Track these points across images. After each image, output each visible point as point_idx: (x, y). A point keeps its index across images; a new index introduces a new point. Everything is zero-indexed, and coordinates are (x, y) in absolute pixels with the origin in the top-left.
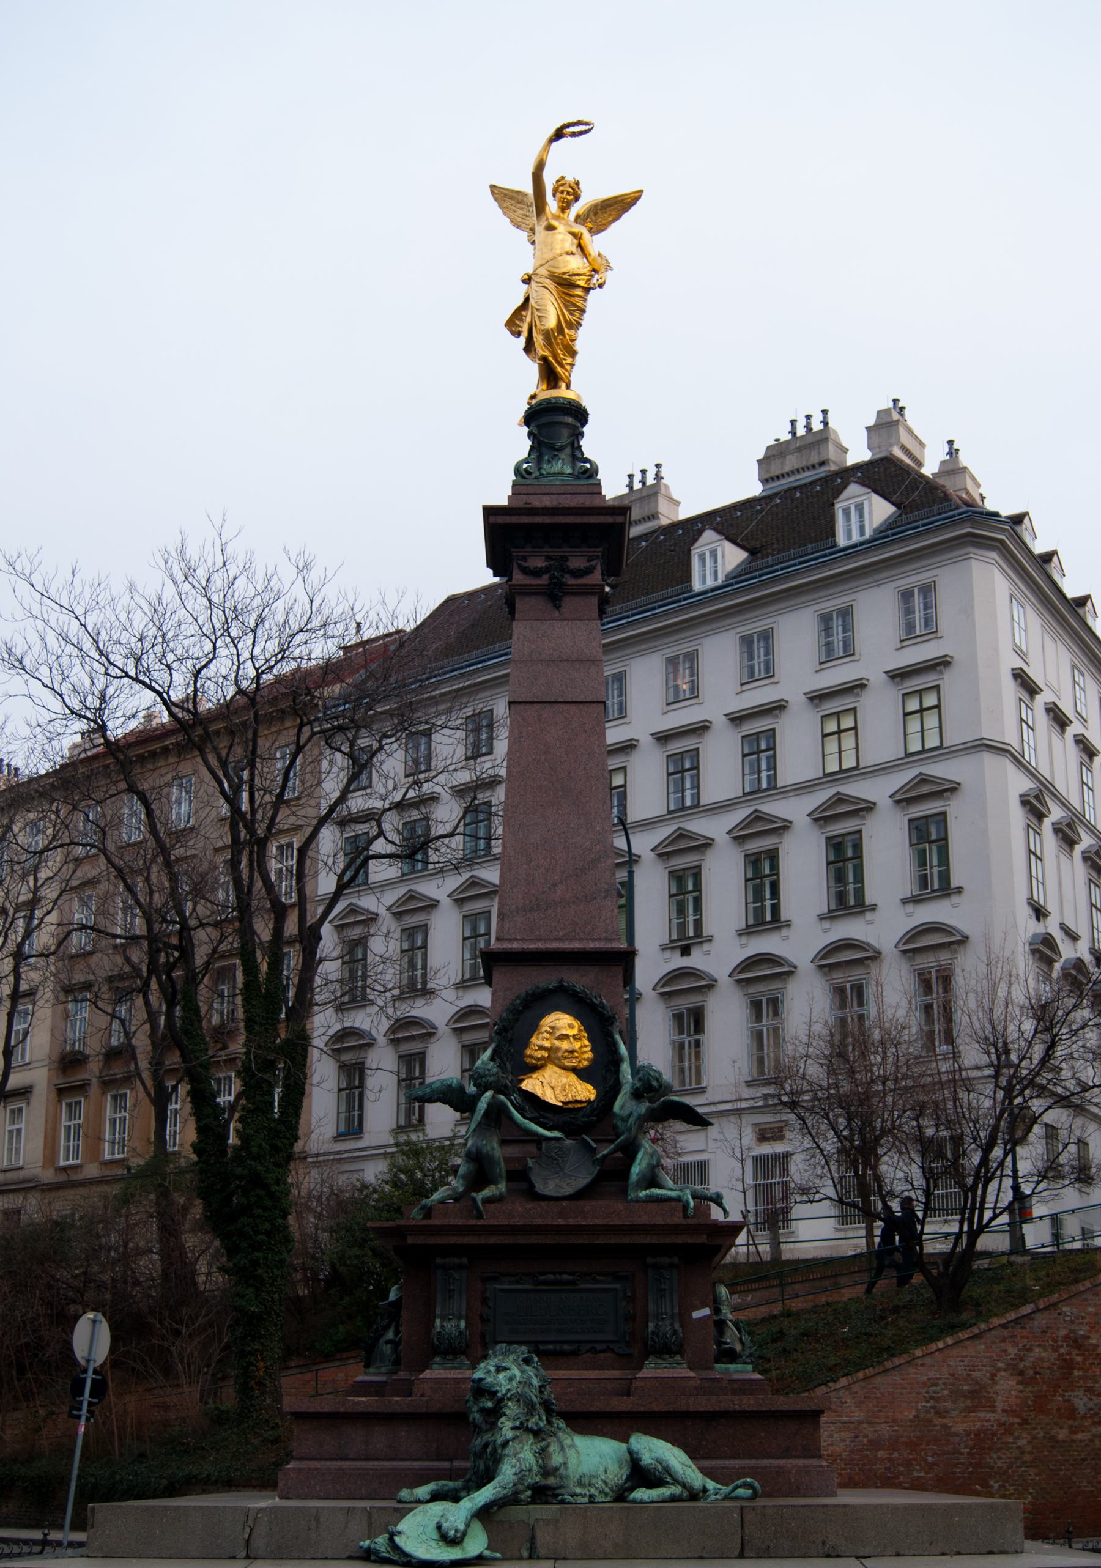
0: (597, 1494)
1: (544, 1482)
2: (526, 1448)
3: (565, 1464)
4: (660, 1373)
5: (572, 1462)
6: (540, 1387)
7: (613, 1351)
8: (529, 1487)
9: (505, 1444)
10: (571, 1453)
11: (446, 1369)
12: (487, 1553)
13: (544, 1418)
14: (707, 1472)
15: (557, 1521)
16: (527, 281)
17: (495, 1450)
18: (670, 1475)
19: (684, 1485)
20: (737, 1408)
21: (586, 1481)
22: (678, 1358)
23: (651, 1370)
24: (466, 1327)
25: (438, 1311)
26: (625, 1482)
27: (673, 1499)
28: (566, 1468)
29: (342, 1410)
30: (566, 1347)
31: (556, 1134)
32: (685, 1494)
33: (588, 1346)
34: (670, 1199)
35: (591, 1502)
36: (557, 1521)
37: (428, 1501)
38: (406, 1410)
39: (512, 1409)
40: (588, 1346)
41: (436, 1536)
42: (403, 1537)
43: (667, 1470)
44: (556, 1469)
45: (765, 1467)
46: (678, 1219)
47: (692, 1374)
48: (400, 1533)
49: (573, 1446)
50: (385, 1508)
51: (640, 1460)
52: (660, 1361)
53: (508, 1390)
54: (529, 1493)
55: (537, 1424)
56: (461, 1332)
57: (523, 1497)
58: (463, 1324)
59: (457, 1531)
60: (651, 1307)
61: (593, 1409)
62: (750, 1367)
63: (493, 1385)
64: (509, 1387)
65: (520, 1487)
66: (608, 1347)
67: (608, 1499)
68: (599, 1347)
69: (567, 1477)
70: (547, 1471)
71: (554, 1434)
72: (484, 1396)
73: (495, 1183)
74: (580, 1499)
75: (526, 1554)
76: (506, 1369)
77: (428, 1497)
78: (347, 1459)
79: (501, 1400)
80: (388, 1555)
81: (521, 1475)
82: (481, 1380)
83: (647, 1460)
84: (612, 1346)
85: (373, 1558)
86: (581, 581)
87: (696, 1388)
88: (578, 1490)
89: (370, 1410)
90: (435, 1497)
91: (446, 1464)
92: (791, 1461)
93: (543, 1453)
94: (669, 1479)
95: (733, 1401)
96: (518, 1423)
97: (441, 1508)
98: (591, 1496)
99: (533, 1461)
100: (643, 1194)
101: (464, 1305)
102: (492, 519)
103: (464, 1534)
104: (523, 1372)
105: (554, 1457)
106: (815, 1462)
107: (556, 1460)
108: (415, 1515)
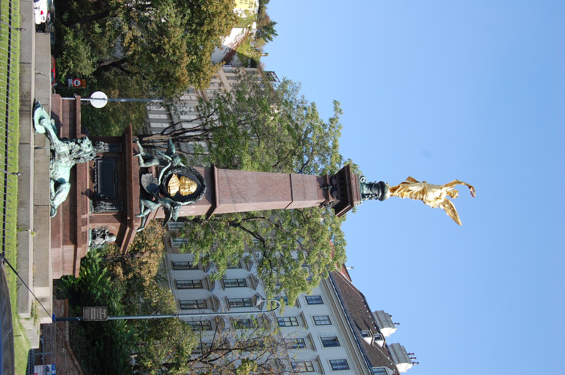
1: (56, 154)
9: (67, 143)
16: (424, 182)
22: (93, 210)
30: (96, 180)
31: (160, 183)
34: (141, 210)
39: (78, 147)
43: (59, 192)
46: (135, 212)
65: (55, 145)
70: (59, 156)
73: (145, 162)
79: (79, 145)
83: (63, 186)
86: (330, 196)
88: (54, 165)
99: (62, 151)
100: (142, 202)
102: (346, 169)
106: (61, 243)
107: (63, 160)
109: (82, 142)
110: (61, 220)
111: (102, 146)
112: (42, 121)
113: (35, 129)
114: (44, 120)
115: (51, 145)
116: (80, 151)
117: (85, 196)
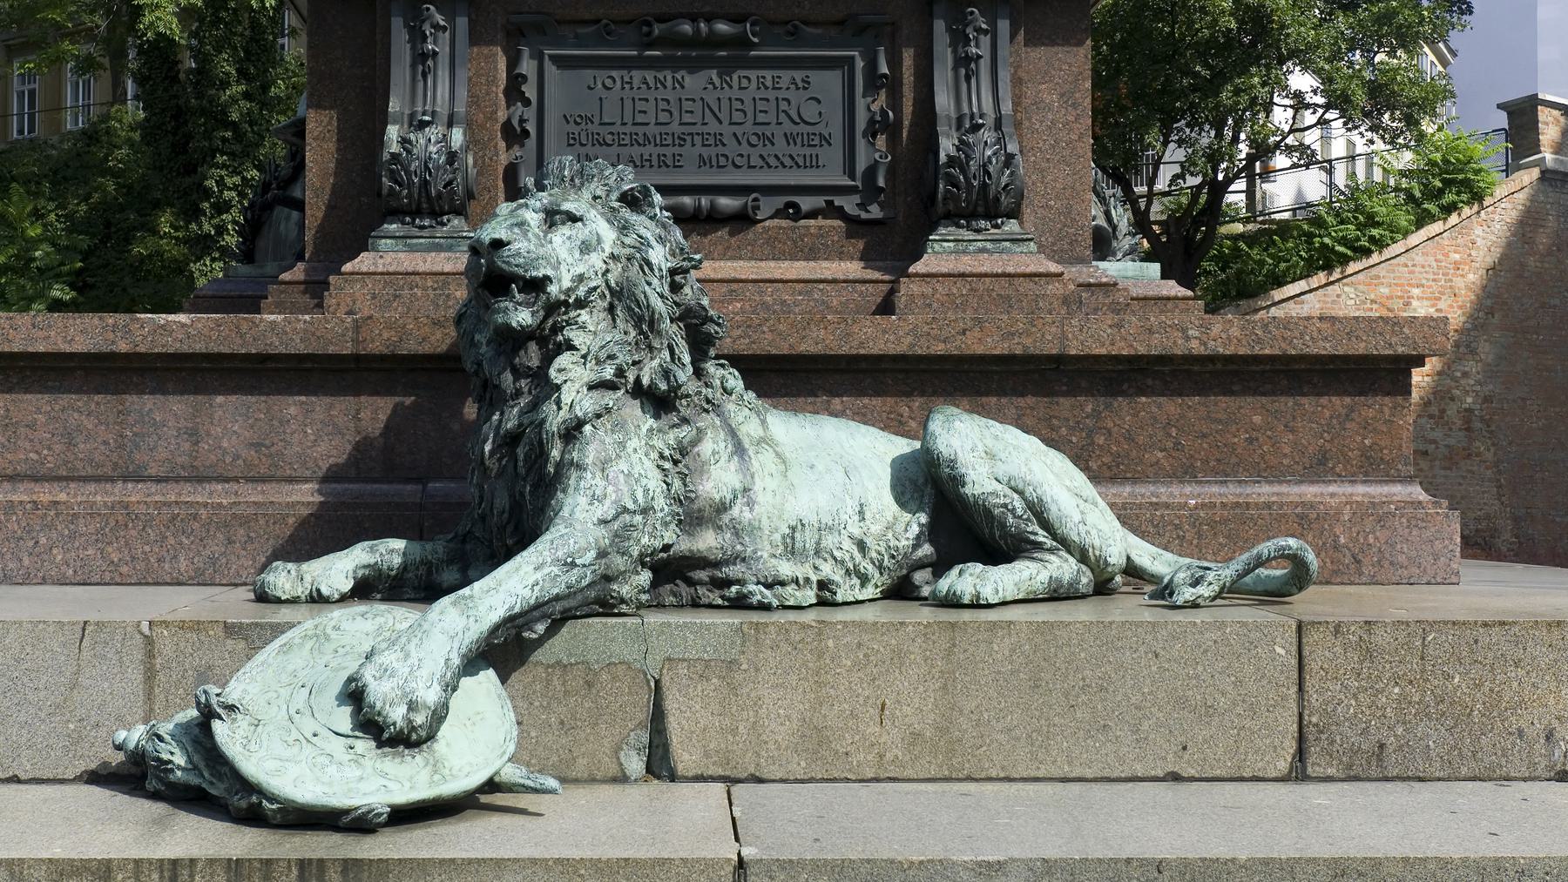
0: (837, 578)
1: (684, 545)
2: (633, 443)
3: (746, 490)
4: (967, 264)
5: (766, 488)
6: (673, 272)
7: (840, 213)
8: (641, 562)
9: (572, 432)
10: (762, 461)
11: (412, 249)
12: (512, 773)
13: (687, 359)
14: (1129, 518)
15: (732, 664)
17: (541, 453)
18: (1046, 525)
19: (1082, 555)
20: (1196, 347)
21: (807, 539)
22: (1012, 226)
23: (944, 253)
24: (466, 148)
25: (394, 105)
26: (916, 547)
27: (1057, 594)
28: (750, 504)
29: (123, 347)
30: (726, 203)
32: (1086, 579)
33: (780, 201)
35: (822, 603)
36: (732, 664)
37: (344, 599)
38: (302, 349)
39: (591, 330)
40: (780, 201)
41: (343, 718)
42: (243, 722)
43: (1038, 511)
44: (722, 507)
45: (1268, 506)
47: (1053, 267)
48: (231, 708)
49: (765, 441)
50: (197, 626)
51: (958, 480)
52: (970, 235)
53: (581, 278)
54: (645, 577)
55: (666, 374)
56: (452, 157)
57: (625, 590)
58: (457, 137)
59: (412, 706)
60: (943, 101)
61: (806, 347)
62: (1155, 268)
63: (533, 262)
64: (580, 269)
65: (619, 562)
66: (830, 203)
67: (870, 592)
68: (806, 203)
69: (754, 529)
70: (692, 516)
71: (711, 406)
72: (506, 292)
74: (792, 595)
75: (635, 764)
76: (573, 219)
77: (347, 586)
78: (139, 478)
80: (194, 780)
81: (619, 528)
82: (498, 244)
83: (980, 481)
84: (838, 201)
85: (152, 784)
87: (1065, 301)
88: (786, 569)
89: (199, 347)
90: (366, 588)
91: (409, 491)
92: (1332, 488)
93: (680, 459)
94: (1042, 536)
95: (1184, 331)
96: (608, 372)
97: (369, 625)
98: (823, 585)
99: (654, 482)
101: (462, 93)
103: (439, 715)
104: (624, 228)
105: (715, 471)
107: (719, 480)
108: (287, 648)
109: (536, 286)
110: (1189, 494)
111: (429, 142)
112: (397, 715)
113: (491, 786)
114: (379, 691)
115: (606, 606)
116: (621, 299)
117: (907, 288)
